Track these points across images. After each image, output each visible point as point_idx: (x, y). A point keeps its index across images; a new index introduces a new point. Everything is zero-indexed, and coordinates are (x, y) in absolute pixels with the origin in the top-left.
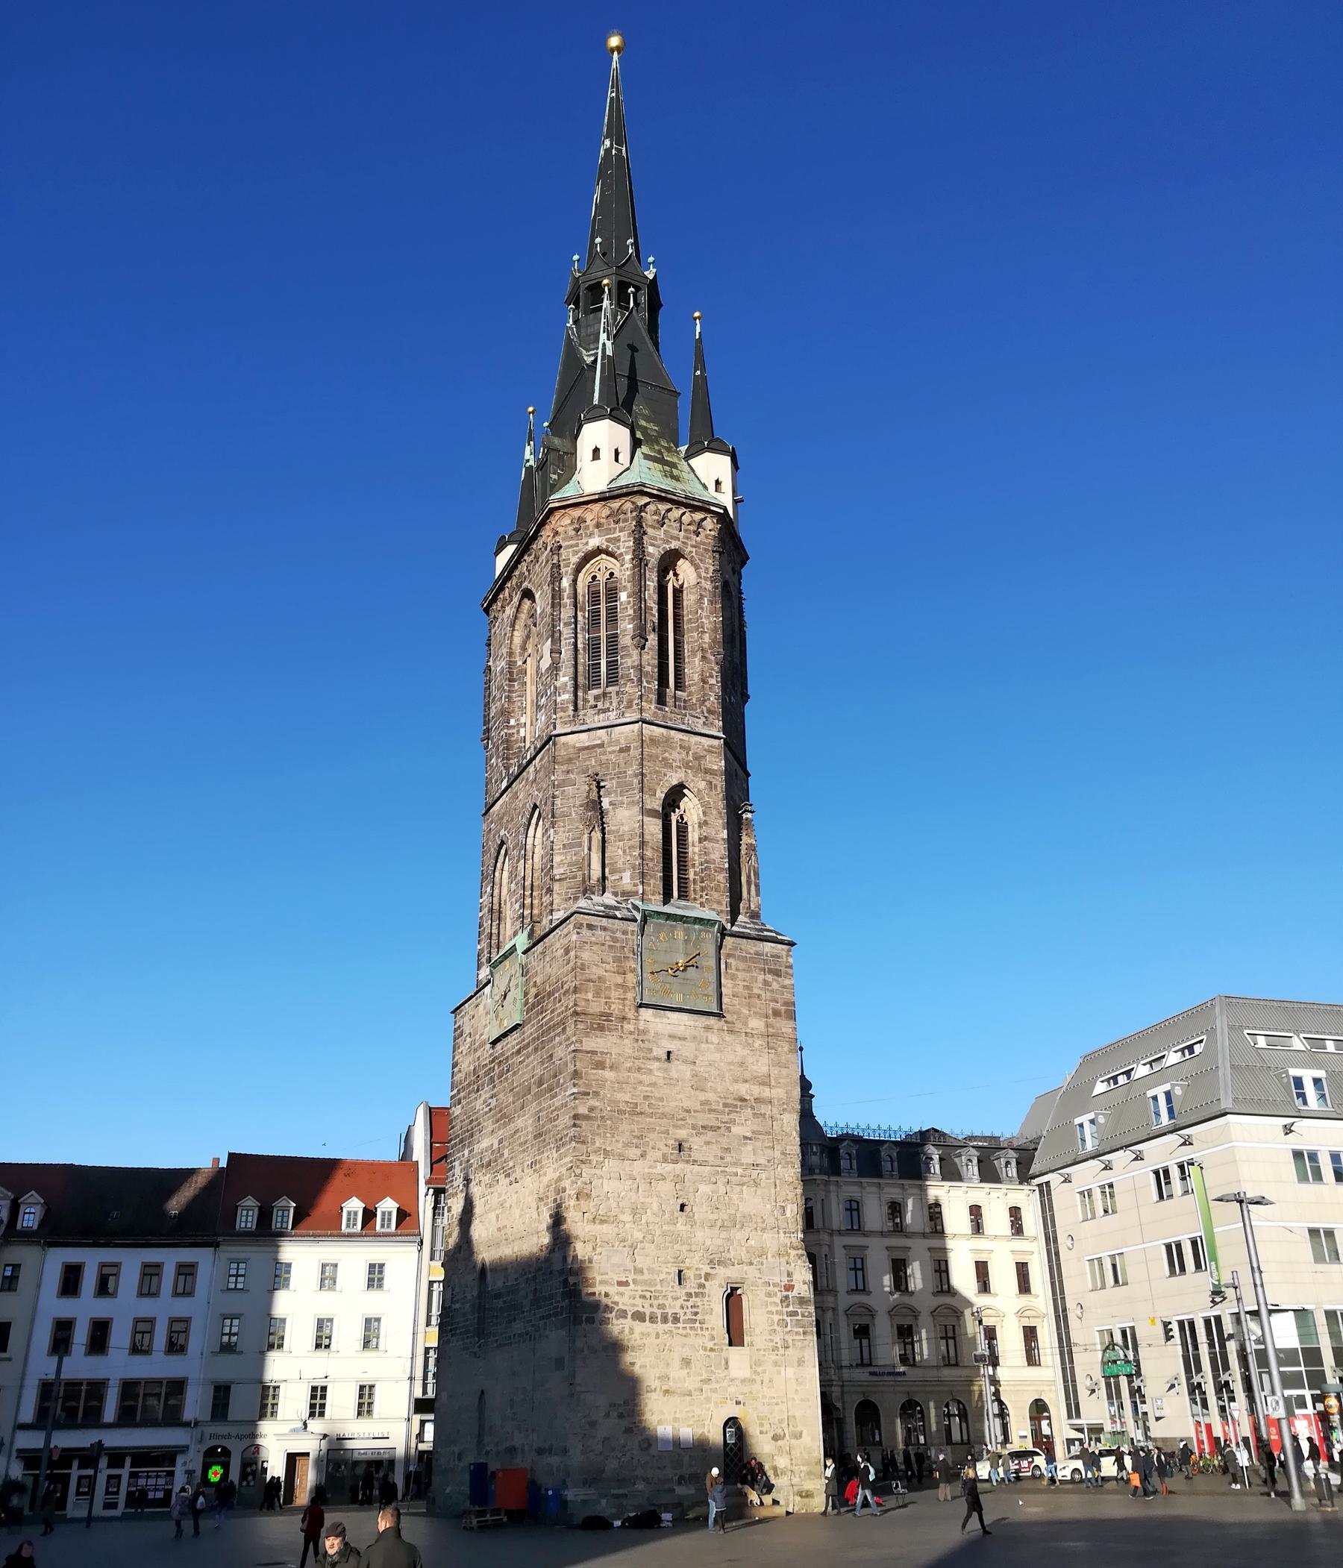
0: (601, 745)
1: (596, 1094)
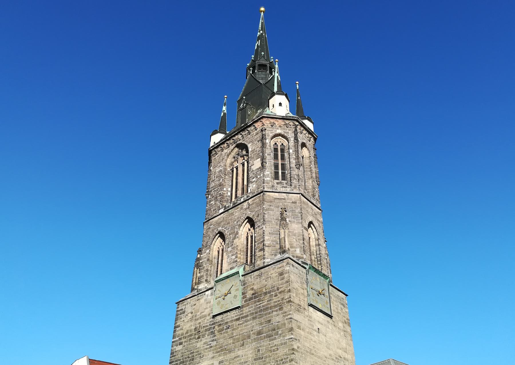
0: (284, 199)
1: (299, 340)
